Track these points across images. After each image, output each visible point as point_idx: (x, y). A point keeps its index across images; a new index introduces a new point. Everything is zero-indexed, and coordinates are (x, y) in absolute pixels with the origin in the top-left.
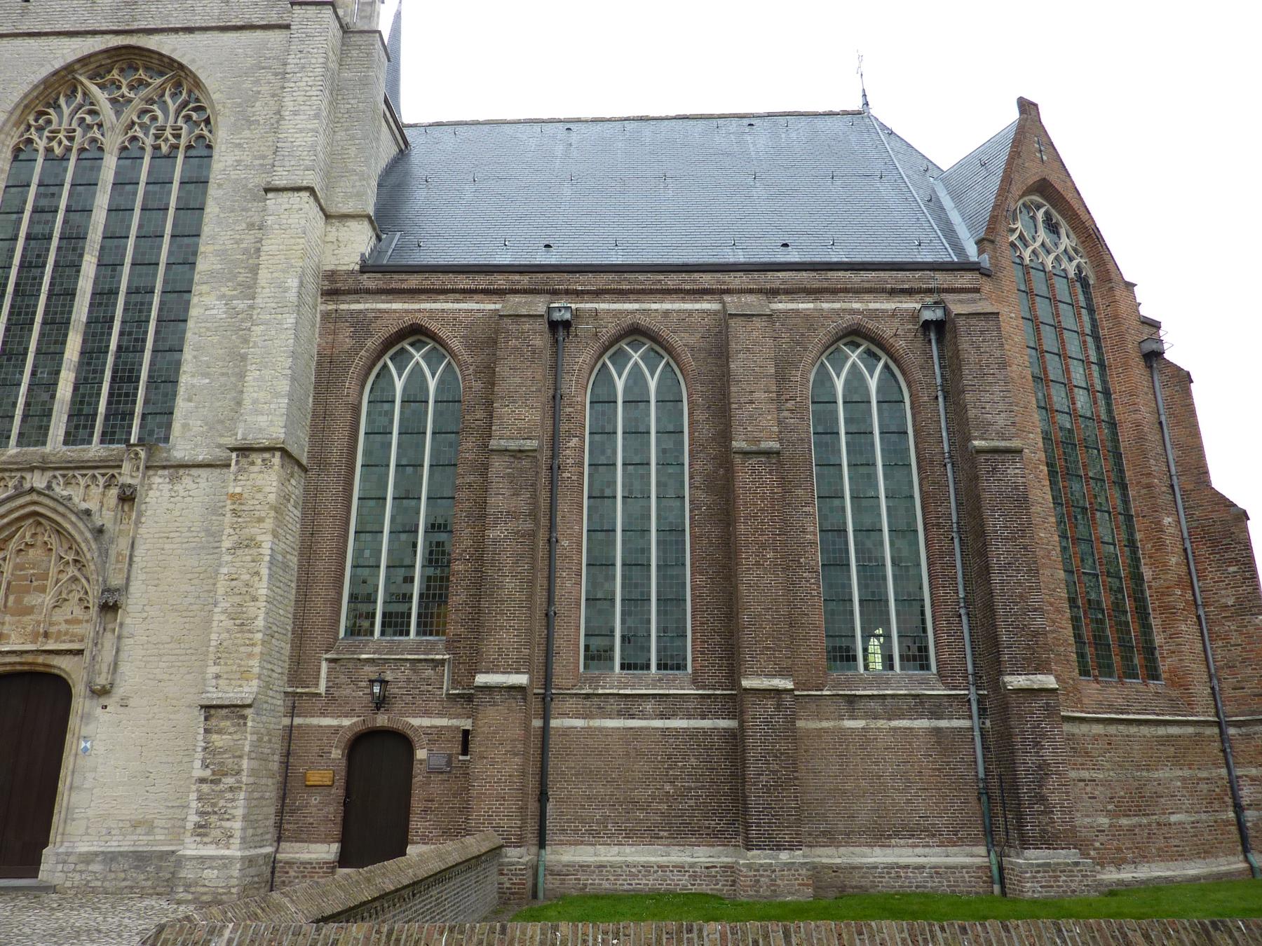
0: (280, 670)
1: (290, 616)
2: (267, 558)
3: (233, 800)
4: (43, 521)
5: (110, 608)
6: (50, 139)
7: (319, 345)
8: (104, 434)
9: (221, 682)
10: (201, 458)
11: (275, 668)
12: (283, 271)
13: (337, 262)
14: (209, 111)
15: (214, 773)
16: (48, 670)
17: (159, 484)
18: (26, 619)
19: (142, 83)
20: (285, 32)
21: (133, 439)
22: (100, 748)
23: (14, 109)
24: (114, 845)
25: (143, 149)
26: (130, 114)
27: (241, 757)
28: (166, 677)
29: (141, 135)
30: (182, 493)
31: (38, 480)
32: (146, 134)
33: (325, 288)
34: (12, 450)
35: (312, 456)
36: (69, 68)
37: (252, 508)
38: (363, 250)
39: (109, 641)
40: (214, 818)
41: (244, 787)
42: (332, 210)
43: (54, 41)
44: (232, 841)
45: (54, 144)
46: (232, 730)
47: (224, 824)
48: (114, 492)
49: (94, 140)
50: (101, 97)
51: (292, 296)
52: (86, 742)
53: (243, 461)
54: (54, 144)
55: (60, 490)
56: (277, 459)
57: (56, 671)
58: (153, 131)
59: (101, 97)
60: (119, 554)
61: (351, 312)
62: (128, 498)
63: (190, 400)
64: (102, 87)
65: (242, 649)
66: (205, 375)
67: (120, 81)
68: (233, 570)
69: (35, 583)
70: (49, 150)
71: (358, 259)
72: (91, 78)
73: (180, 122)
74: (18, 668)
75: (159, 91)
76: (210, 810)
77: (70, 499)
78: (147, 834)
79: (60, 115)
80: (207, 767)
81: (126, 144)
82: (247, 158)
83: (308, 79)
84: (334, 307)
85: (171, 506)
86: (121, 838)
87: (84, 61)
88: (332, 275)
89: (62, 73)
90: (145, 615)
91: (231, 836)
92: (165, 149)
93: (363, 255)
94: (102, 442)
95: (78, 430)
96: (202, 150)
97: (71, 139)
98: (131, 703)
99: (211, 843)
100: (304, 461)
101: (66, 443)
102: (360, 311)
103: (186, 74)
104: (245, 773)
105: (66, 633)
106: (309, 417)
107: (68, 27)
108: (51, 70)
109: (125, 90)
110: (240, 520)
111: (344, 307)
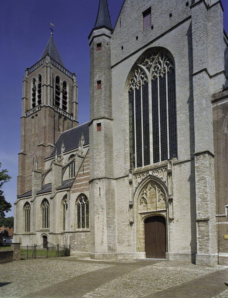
1: (215, 196)
4: (153, 182)
5: (171, 200)
6: (135, 86)
7: (213, 119)
8: (162, 158)
9: (200, 215)
11: (213, 210)
13: (215, 90)
14: (171, 59)
15: (202, 236)
16: (160, 215)
17: (177, 168)
19: (153, 59)
21: (169, 158)
23: (126, 81)
24: (181, 252)
26: (152, 69)
27: (208, 232)
28: (186, 214)
29: (156, 74)
30: (182, 169)
31: (150, 173)
32: (157, 74)
33: (213, 100)
34: (143, 167)
36: (136, 64)
37: (202, 169)
38: (223, 84)
40: (203, 247)
43: (131, 58)
45: (137, 86)
46: (205, 226)
49: (145, 82)
50: (144, 68)
52: (171, 230)
53: (198, 157)
54: (137, 86)
55: (155, 174)
57: (161, 215)
58: (158, 72)
59: (144, 68)
61: (222, 105)
63: (180, 144)
64: (144, 65)
65: (205, 206)
66: (184, 136)
67: (148, 61)
68: (199, 186)
69: (154, 196)
70: (136, 89)
71: (222, 87)
72: (141, 64)
73: (165, 65)
75: (158, 59)
76: (202, 245)
77: (157, 176)
79: (136, 78)
80: (200, 235)
81: (153, 79)
83: (199, 32)
84: (216, 105)
86: (182, 251)
87: (138, 60)
88: (214, 95)
89: (134, 66)
90: (179, 200)
92: (162, 75)
95: (156, 160)
97: (140, 84)
101: (154, 163)
102: (224, 104)
103: (164, 50)
104: (210, 236)
105: (162, 207)
106: (213, 140)
107: (133, 51)
108: (132, 66)
109: (149, 63)
110: (199, 173)
111: (220, 104)
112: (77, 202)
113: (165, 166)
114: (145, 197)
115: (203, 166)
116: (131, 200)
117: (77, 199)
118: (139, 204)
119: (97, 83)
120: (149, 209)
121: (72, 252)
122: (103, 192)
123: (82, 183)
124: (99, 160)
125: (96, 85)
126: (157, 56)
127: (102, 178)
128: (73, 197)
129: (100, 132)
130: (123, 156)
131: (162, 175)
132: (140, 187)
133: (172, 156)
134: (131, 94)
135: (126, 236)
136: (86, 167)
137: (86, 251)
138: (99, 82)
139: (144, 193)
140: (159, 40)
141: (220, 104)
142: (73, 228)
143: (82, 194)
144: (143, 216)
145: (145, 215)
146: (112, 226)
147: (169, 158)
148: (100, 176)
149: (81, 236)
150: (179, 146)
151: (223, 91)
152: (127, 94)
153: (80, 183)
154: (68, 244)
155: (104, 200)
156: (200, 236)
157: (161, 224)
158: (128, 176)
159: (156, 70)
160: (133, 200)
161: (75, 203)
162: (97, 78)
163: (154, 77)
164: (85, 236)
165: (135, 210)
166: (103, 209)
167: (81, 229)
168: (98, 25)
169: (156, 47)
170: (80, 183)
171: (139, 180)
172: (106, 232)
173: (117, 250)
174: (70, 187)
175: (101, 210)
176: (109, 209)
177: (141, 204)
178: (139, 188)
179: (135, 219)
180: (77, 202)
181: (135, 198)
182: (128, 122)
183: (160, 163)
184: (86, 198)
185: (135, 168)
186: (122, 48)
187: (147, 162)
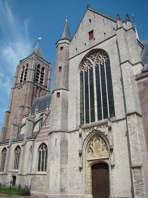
0: (146, 158)
2: (138, 135)
3: (142, 187)
5: (111, 150)
6: (85, 70)
10: (121, 118)
11: (145, 158)
12: (127, 78)
18: (98, 153)
19: (96, 55)
20: (116, 36)
21: (109, 117)
22: (115, 177)
25: (99, 66)
27: (142, 177)
29: (98, 63)
30: (119, 125)
31: (95, 128)
34: (90, 123)
35: (142, 113)
39: (112, 156)
40: (139, 191)
41: (144, 184)
42: (133, 63)
44: (144, 196)
47: (142, 192)
48: (108, 128)
49: (91, 67)
50: (90, 60)
51: (130, 82)
53: (129, 116)
55: (99, 129)
56: (135, 115)
58: (99, 62)
59: (90, 60)
60: (111, 139)
61: (142, 82)
62: (110, 129)
63: (117, 107)
64: (90, 58)
65: (137, 155)
66: (118, 102)
68: (132, 139)
70: (85, 71)
73: (103, 58)
74: (99, 162)
78: (127, 194)
79: (85, 65)
82: (116, 60)
85: (118, 128)
87: (86, 55)
88: (136, 76)
90: (118, 150)
91: (144, 195)
93: (141, 70)
94: (104, 119)
95: (100, 118)
96: (108, 62)
97: (87, 68)
98: (119, 167)
99: (140, 196)
100: (141, 114)
101: (98, 120)
102: (144, 81)
104: (144, 181)
105: (105, 155)
108: (82, 59)
109: (93, 57)
111: (141, 81)
112: (39, 150)
113: (106, 123)
114: (92, 147)
115: (133, 123)
116: (81, 149)
117: (39, 147)
118: (87, 153)
119: (59, 68)
120: (95, 157)
121: (32, 192)
122: (58, 142)
123: (44, 134)
124: (56, 118)
125: (58, 69)
126: (98, 54)
127: (58, 132)
128: (37, 145)
129: (58, 98)
130: (75, 116)
131: (104, 130)
132: (88, 139)
133: (111, 115)
134: (81, 74)
135: (76, 180)
136: (48, 123)
137: (43, 192)
138: (60, 68)
139: (90, 144)
140: (99, 45)
141: (141, 81)
142: (34, 171)
143: (43, 143)
144: (90, 163)
145: (92, 162)
146: (65, 171)
147: (109, 117)
148: (57, 130)
149: (40, 178)
150: (116, 109)
151: (142, 73)
152: (79, 74)
153: (43, 135)
154: (29, 185)
155: (59, 148)
156: (136, 181)
157: (105, 170)
158: (78, 130)
159: (98, 60)
160: (82, 149)
161: (37, 150)
162: (59, 65)
163: (97, 64)
164: (43, 178)
165: (84, 157)
166: (58, 156)
167: (40, 172)
168: (62, 38)
169: (97, 49)
170: (43, 135)
171: (87, 133)
172: (59, 176)
173: (69, 192)
174: (35, 138)
175: (56, 157)
176: (63, 156)
177: (88, 153)
178: (87, 139)
179: (84, 165)
180: (39, 150)
181: (83, 148)
182: (80, 92)
183: (103, 120)
184: (46, 147)
185: (84, 124)
186: (76, 49)
187: (93, 120)
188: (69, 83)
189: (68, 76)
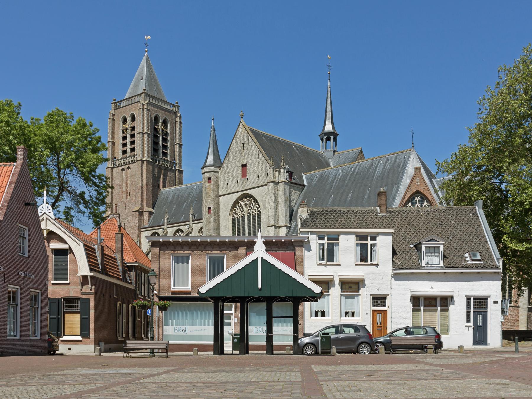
6: (237, 215)
50: (243, 204)
59: (243, 204)
87: (239, 198)
119: (208, 209)
134: (234, 219)
138: (210, 208)
152: (231, 220)
162: (208, 205)
188: (221, 228)
189: (218, 220)
